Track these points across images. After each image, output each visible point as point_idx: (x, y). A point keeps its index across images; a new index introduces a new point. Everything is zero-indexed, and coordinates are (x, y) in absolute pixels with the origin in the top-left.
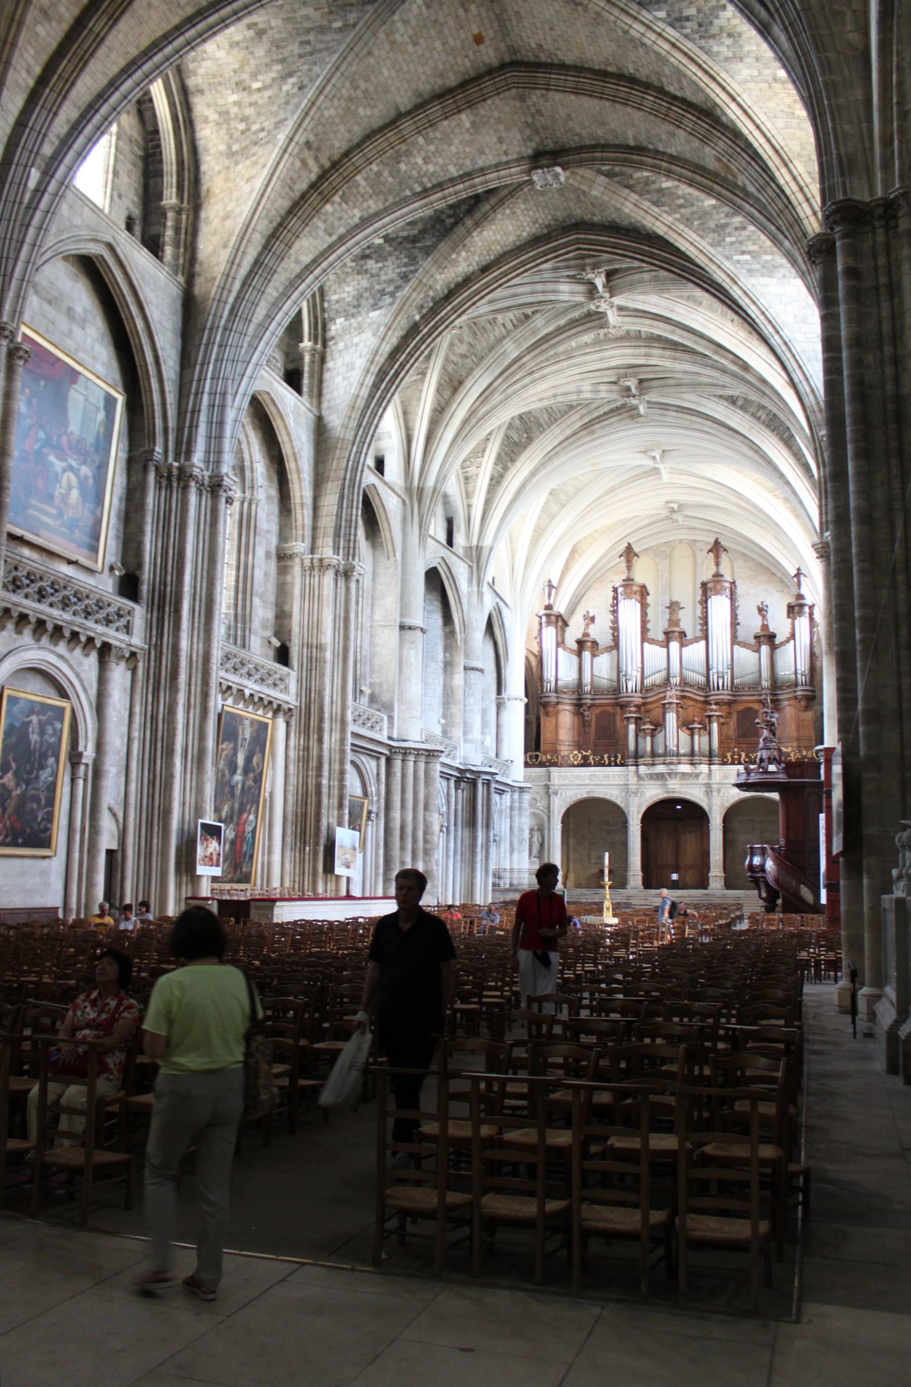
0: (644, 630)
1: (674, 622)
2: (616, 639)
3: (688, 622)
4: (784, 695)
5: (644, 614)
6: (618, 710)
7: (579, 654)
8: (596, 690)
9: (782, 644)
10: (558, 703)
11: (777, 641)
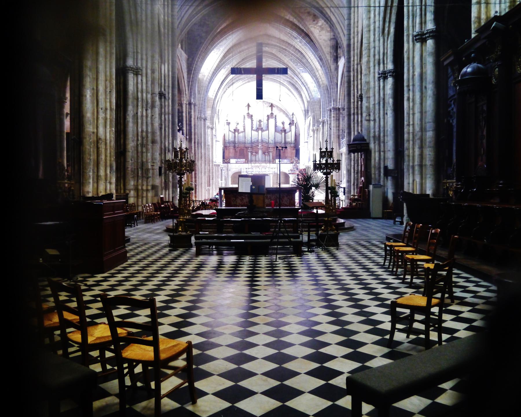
0: (252, 127)
1: (260, 125)
2: (244, 129)
3: (264, 125)
5: (252, 123)
6: (245, 148)
7: (234, 133)
8: (239, 143)
10: (229, 146)
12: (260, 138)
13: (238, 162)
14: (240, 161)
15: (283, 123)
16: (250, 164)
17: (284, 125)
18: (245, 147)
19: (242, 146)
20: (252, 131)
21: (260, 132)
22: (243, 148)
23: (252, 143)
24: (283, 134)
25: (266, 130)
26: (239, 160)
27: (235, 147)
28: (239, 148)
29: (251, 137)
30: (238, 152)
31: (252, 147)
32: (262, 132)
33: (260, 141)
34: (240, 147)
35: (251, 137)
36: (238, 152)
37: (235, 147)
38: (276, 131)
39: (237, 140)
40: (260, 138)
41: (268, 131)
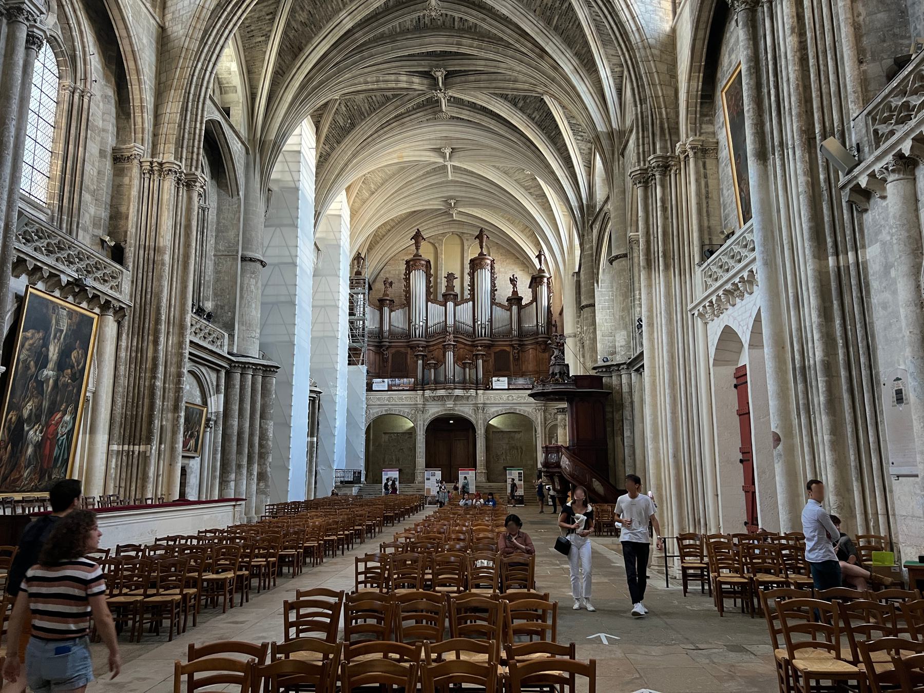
1: (450, 287)
4: (528, 341)
11: (523, 303)
12: (450, 321)
13: (394, 388)
14: (399, 385)
15: (513, 281)
16: (420, 392)
17: (515, 286)
18: (408, 346)
19: (400, 343)
20: (429, 303)
21: (450, 305)
22: (403, 350)
23: (428, 335)
24: (515, 308)
25: (467, 301)
27: (381, 347)
28: (393, 350)
31: (427, 346)
32: (456, 305)
33: (450, 330)
34: (396, 347)
35: (427, 320)
37: (381, 347)
38: (493, 302)
39: (386, 327)
40: (450, 321)
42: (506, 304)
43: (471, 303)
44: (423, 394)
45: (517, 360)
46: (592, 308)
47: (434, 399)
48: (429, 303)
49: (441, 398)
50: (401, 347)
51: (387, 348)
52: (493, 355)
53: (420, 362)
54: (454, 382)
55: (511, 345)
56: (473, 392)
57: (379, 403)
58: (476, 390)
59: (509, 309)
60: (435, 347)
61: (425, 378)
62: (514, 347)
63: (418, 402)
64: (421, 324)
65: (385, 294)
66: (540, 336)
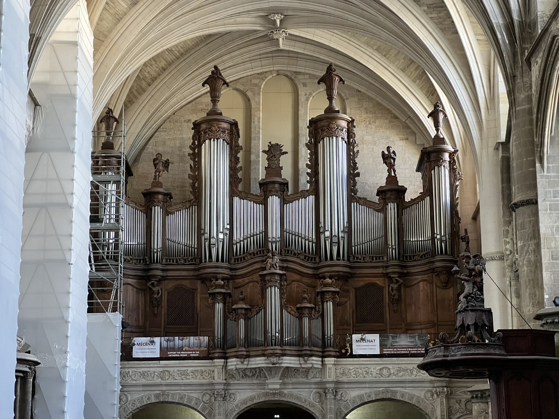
9: (414, 201)
11: (408, 197)
12: (274, 232)
13: (171, 354)
14: (181, 349)
20: (236, 199)
21: (274, 201)
24: (392, 208)
25: (304, 194)
26: (177, 341)
29: (231, 230)
30: (164, 303)
31: (233, 278)
32: (284, 201)
35: (231, 230)
36: (164, 303)
40: (274, 232)
41: (311, 199)
42: (376, 199)
43: (311, 198)
44: (225, 366)
45: (396, 301)
46: (532, 207)
47: (245, 373)
48: (236, 199)
49: (258, 373)
50: (184, 278)
51: (159, 281)
52: (352, 295)
53: (219, 307)
54: (282, 343)
55: (386, 275)
56: (315, 361)
57: (143, 381)
58: (323, 357)
59: (383, 210)
60: (246, 280)
61: (229, 337)
62: (390, 279)
63: (217, 380)
64: (221, 236)
65: (156, 183)
66: (438, 258)
